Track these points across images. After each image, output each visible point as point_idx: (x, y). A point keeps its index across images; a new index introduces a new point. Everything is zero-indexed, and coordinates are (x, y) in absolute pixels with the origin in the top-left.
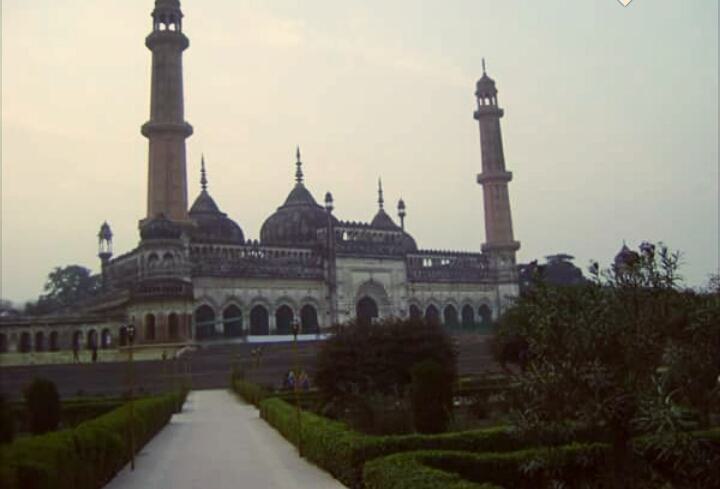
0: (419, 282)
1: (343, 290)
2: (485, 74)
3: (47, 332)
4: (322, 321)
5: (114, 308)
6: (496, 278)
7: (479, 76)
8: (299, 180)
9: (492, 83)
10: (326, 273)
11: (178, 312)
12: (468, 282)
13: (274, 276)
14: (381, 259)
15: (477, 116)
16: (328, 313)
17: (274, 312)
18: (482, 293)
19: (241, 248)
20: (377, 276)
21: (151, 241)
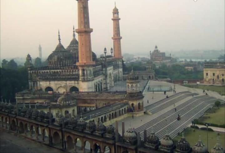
2: (115, 7)
3: (114, 112)
7: (114, 8)
8: (74, 37)
9: (117, 10)
10: (104, 72)
21: (136, 81)
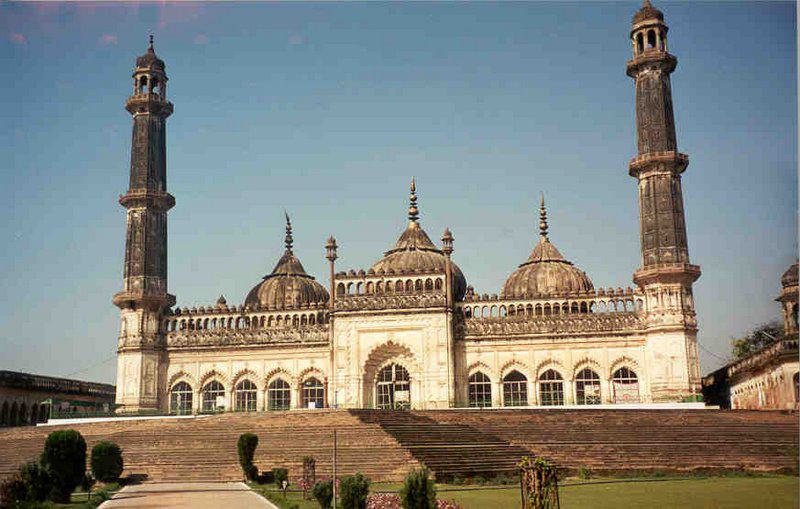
0: (489, 339)
12: (587, 336)
20: (400, 338)
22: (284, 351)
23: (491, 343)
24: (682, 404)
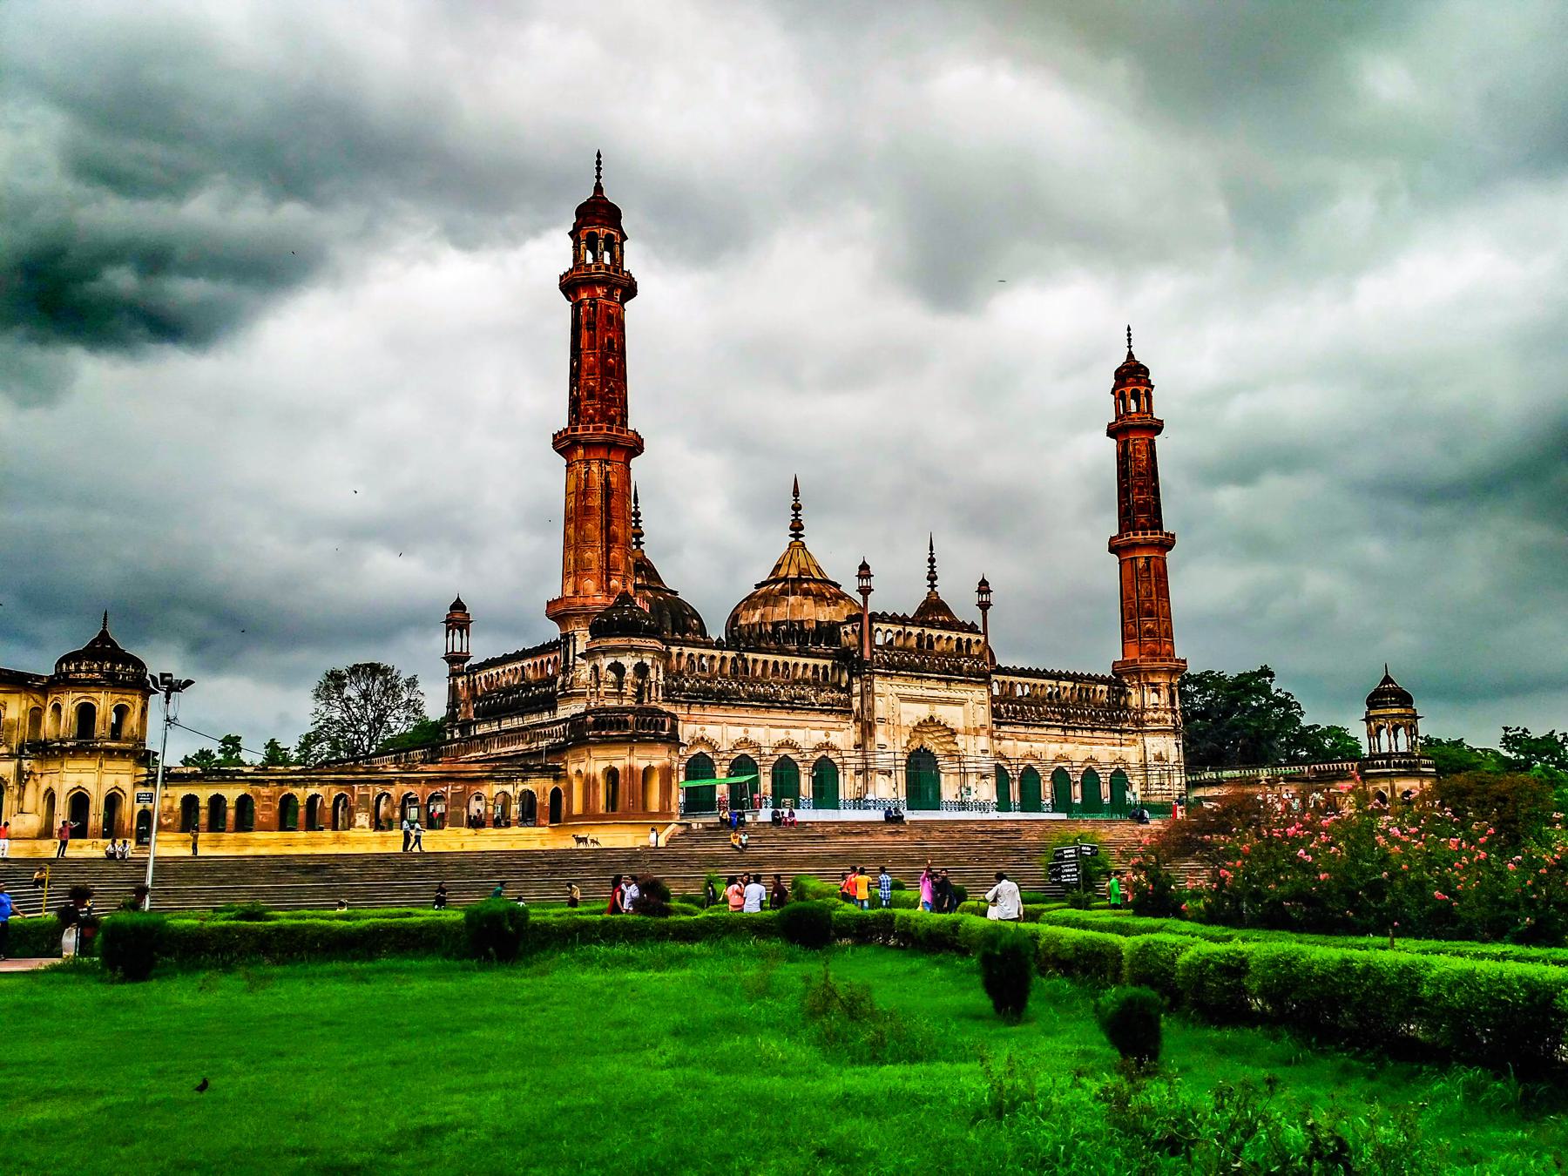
1: (886, 733)
2: (1130, 355)
4: (847, 786)
5: (537, 754)
6: (1140, 722)
8: (797, 536)
11: (655, 764)
12: (1093, 730)
13: (770, 703)
14: (948, 681)
15: (1112, 432)
16: (858, 773)
17: (768, 769)
18: (1117, 748)
19: (717, 653)
20: (944, 713)
21: (613, 642)
22: (792, 716)
23: (1012, 729)
24: (857, 811)
